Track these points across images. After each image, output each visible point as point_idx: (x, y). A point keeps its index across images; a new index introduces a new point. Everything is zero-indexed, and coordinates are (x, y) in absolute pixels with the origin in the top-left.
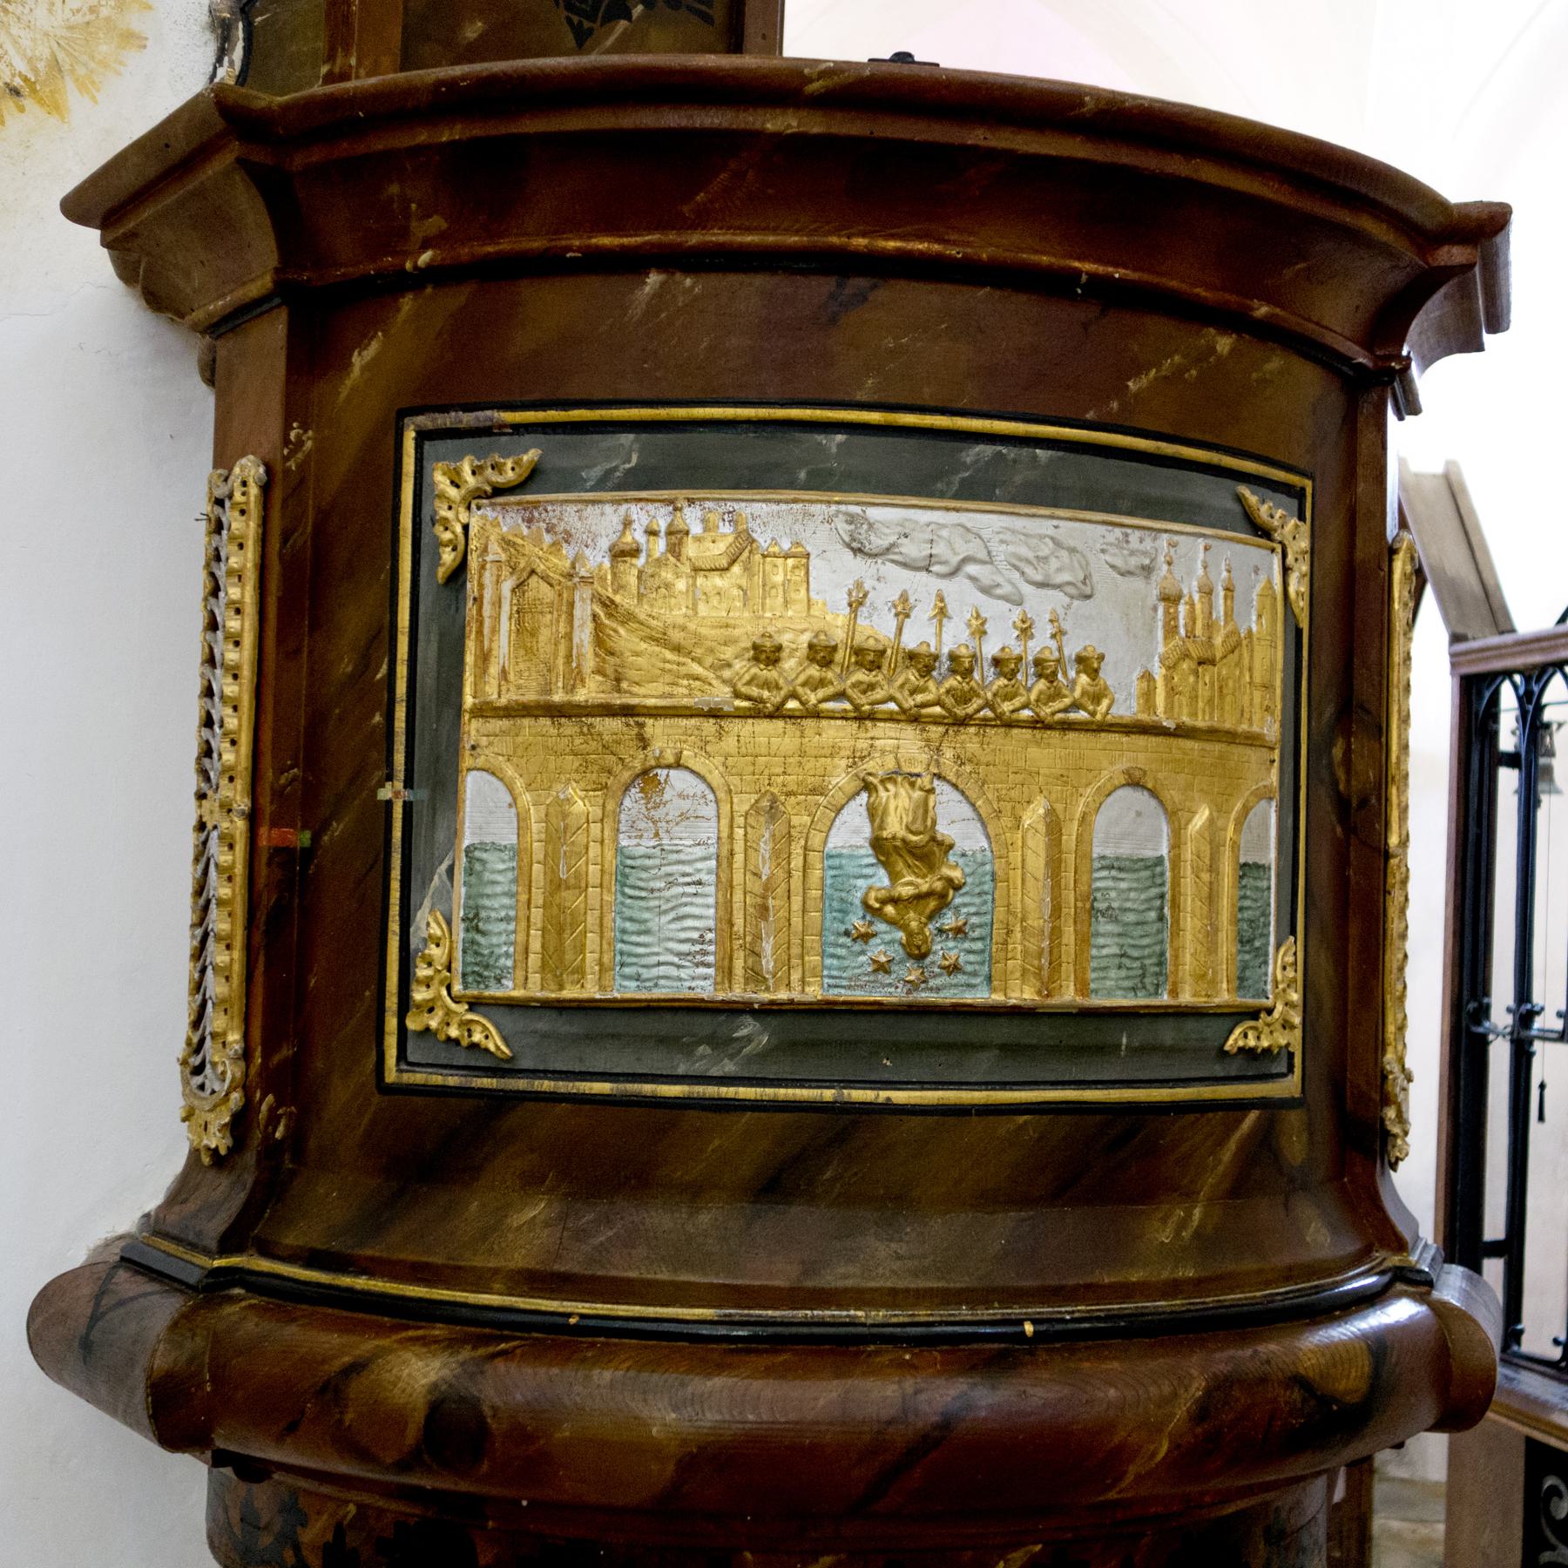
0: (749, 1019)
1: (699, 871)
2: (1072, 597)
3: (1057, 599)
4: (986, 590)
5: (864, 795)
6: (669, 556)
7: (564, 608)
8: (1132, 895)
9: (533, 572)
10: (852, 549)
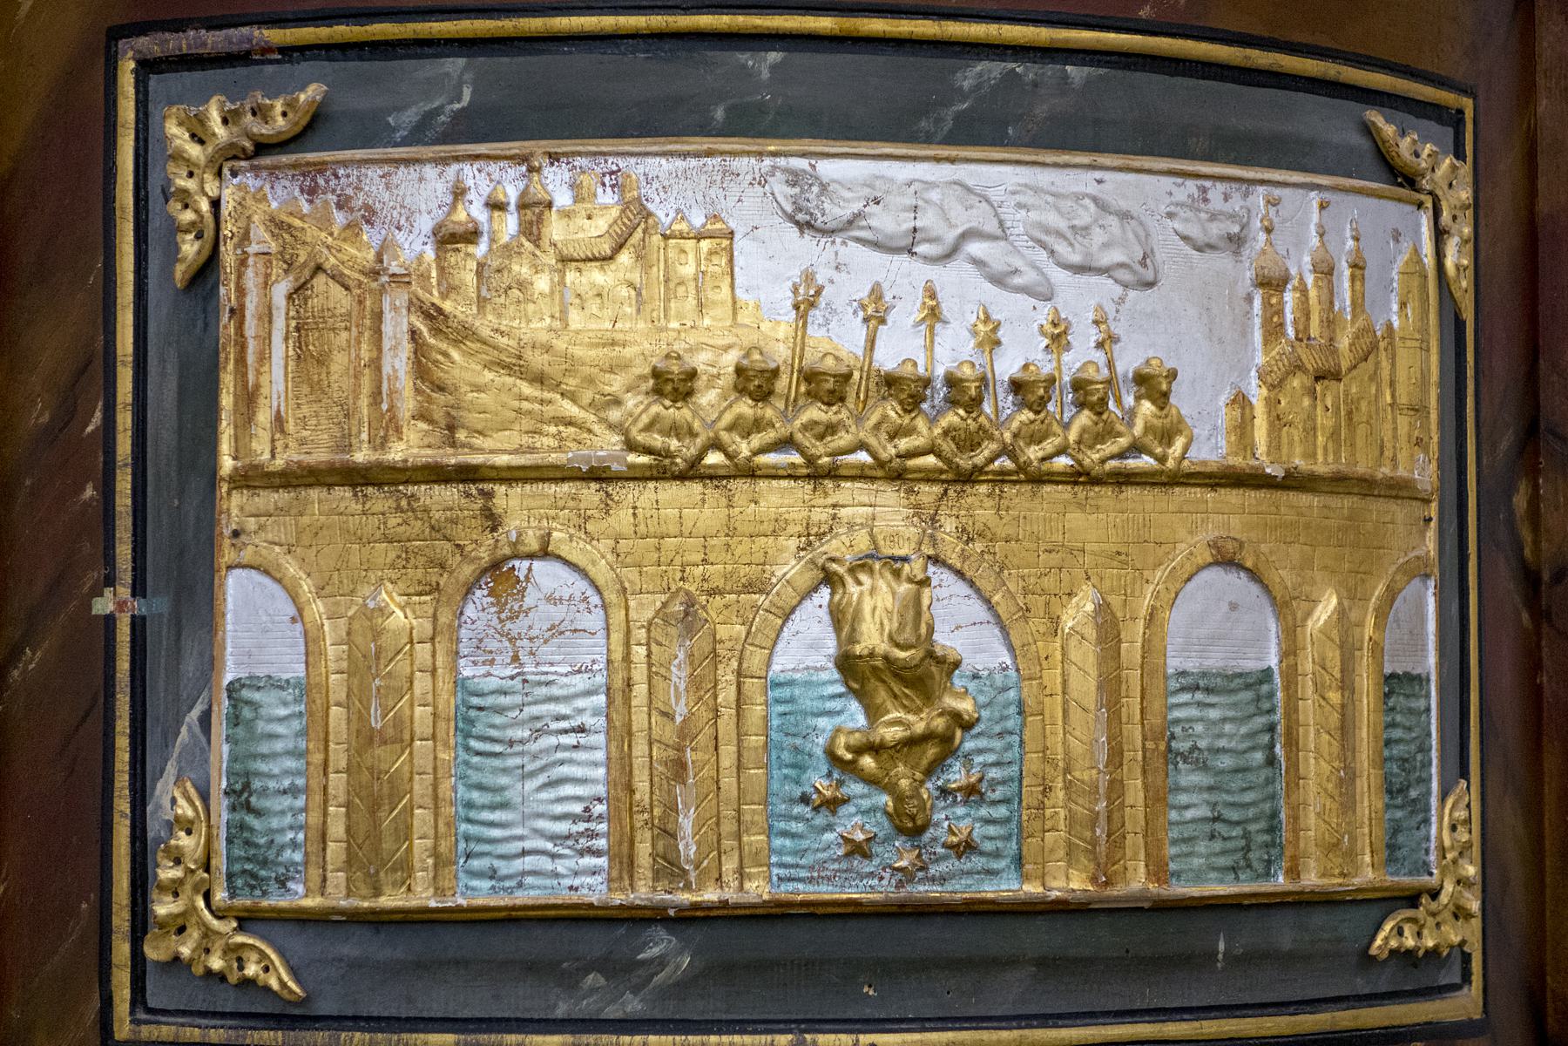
0: (661, 932)
1: (580, 711)
2: (1126, 286)
3: (1105, 288)
4: (998, 280)
5: (825, 592)
6: (523, 240)
7: (368, 322)
8: (1228, 728)
9: (319, 268)
10: (797, 223)
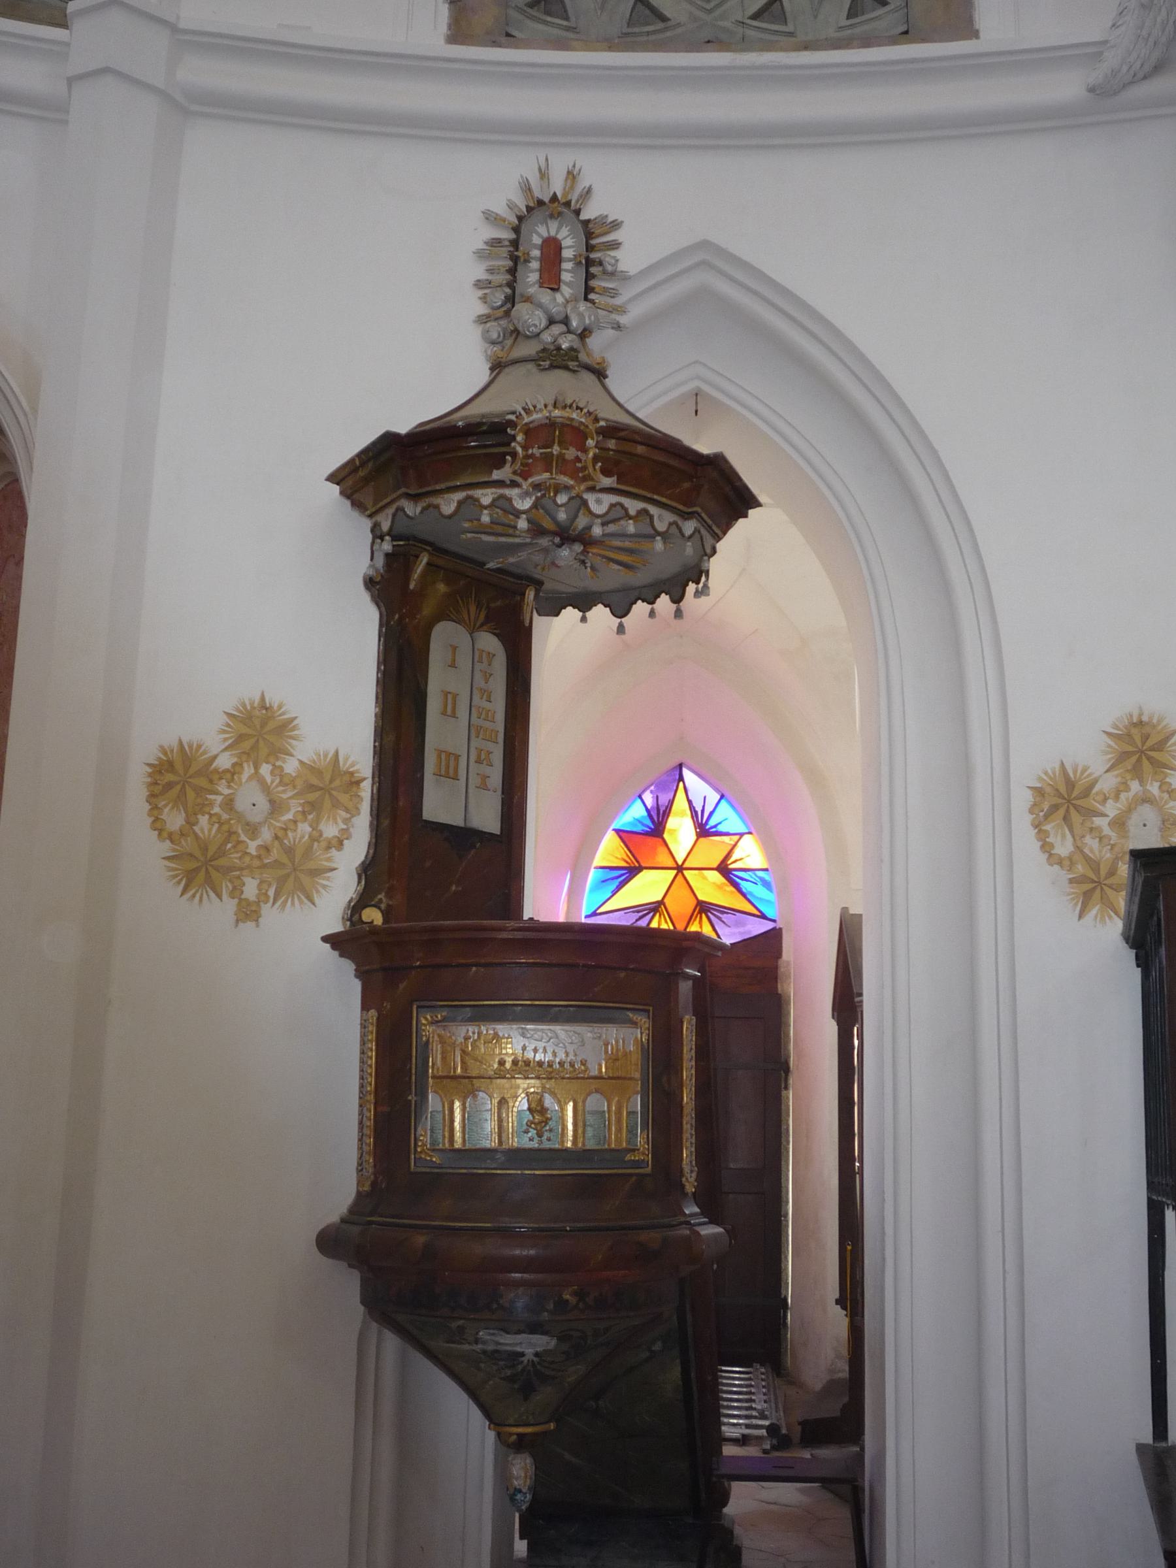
3: (575, 1046)
